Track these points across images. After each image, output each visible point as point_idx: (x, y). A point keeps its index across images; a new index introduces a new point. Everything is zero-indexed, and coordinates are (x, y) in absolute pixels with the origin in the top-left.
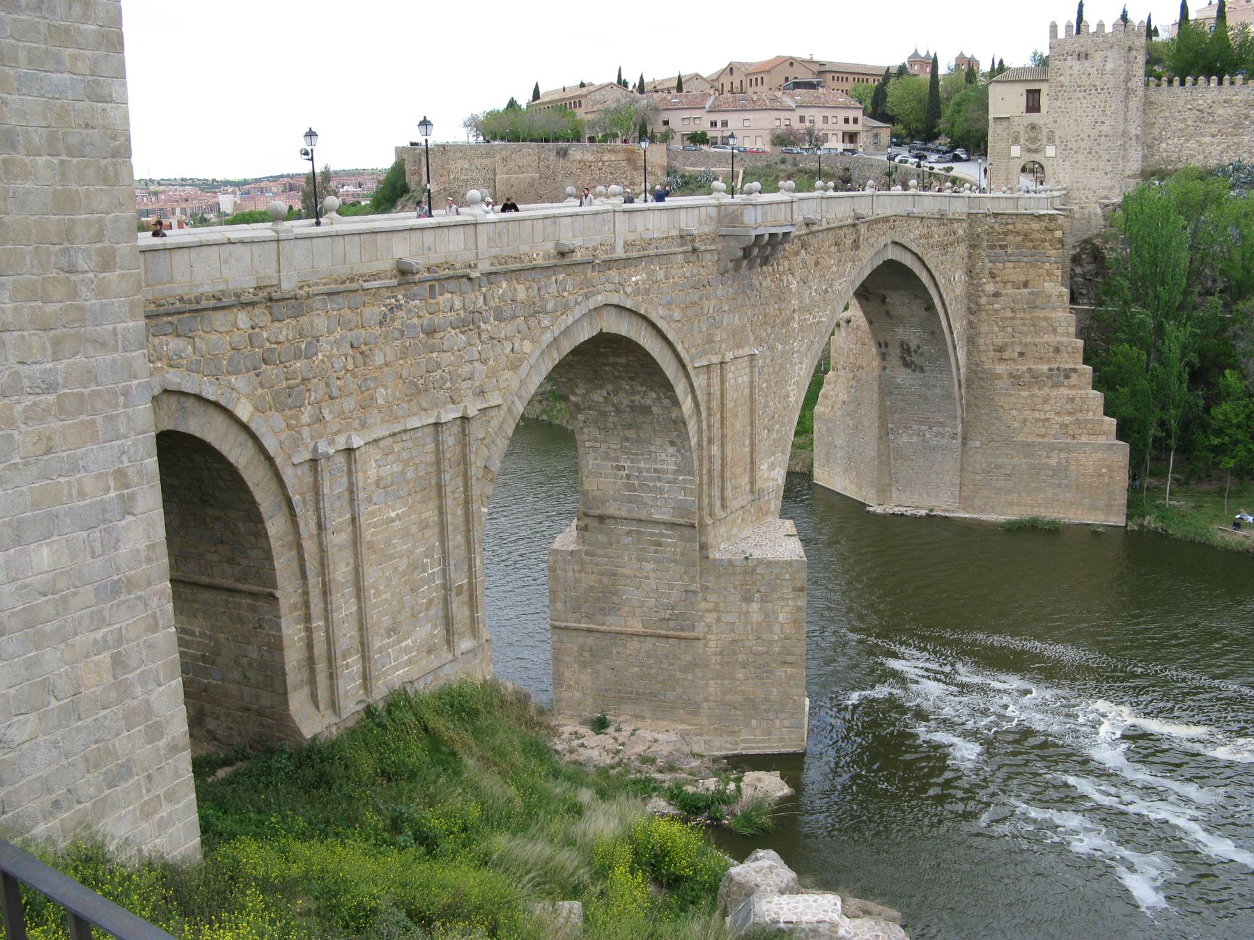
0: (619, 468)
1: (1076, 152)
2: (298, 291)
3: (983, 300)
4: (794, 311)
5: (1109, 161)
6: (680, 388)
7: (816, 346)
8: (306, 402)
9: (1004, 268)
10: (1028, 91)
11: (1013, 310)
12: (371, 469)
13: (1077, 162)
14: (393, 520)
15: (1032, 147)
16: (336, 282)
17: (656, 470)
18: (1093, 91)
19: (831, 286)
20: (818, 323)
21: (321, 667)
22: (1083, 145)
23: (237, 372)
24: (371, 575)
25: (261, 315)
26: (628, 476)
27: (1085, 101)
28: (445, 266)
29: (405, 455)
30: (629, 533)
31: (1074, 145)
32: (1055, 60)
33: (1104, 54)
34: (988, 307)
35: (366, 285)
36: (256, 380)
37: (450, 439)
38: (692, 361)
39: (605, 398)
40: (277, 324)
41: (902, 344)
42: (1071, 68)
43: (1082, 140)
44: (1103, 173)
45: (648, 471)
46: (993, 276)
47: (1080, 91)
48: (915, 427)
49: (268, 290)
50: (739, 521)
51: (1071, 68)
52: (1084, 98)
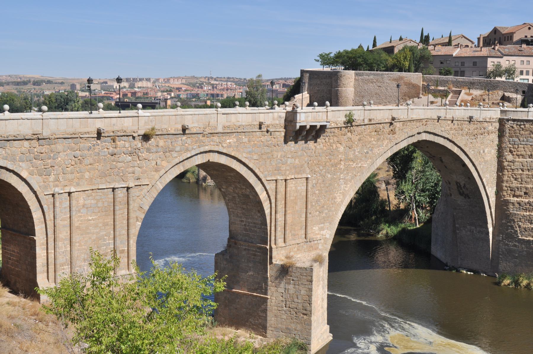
0: (242, 221)
2: (50, 136)
3: (506, 164)
4: (341, 160)
6: (259, 188)
7: (358, 178)
8: (52, 174)
9: (518, 147)
11: (523, 170)
12: (79, 200)
14: (90, 220)
16: (68, 134)
17: (254, 223)
19: (372, 150)
20: (360, 167)
21: (51, 267)
23: (23, 161)
24: (76, 238)
25: (35, 143)
26: (245, 225)
28: (122, 131)
29: (98, 197)
30: (245, 249)
34: (508, 167)
35: (81, 136)
36: (30, 165)
37: (121, 194)
38: (265, 177)
39: (233, 190)
40: (41, 147)
41: (457, 183)
45: (252, 223)
46: (511, 151)
48: (468, 227)
49: (38, 135)
50: (296, 249)
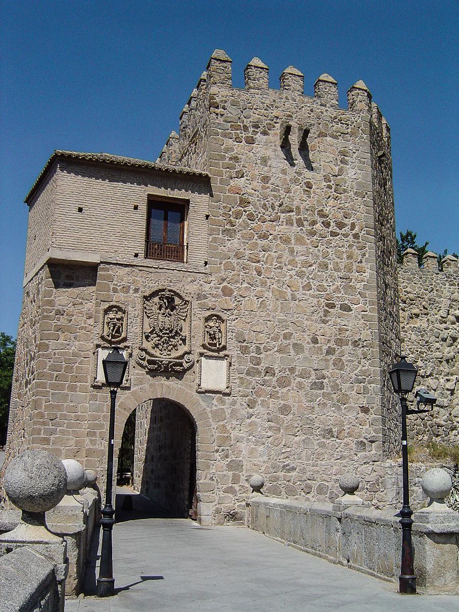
1: (283, 383)
5: (365, 410)
10: (154, 203)
13: (285, 410)
15: (164, 357)
18: (319, 226)
22: (299, 362)
27: (298, 248)
31: (273, 359)
32: (225, 135)
33: (340, 143)
42: (265, 161)
43: (298, 347)
44: (352, 442)
47: (289, 222)
51: (265, 161)
52: (300, 240)
